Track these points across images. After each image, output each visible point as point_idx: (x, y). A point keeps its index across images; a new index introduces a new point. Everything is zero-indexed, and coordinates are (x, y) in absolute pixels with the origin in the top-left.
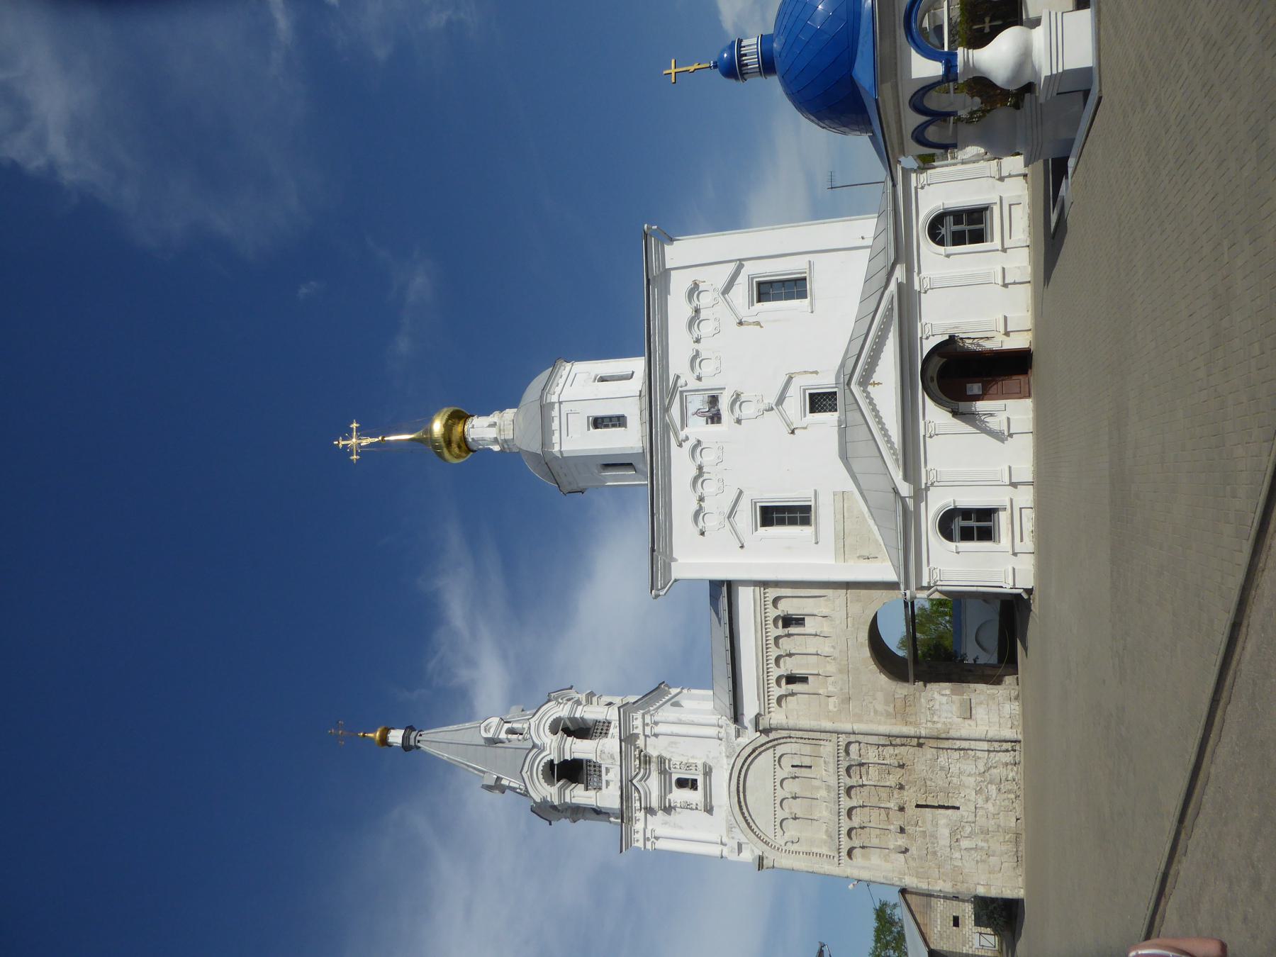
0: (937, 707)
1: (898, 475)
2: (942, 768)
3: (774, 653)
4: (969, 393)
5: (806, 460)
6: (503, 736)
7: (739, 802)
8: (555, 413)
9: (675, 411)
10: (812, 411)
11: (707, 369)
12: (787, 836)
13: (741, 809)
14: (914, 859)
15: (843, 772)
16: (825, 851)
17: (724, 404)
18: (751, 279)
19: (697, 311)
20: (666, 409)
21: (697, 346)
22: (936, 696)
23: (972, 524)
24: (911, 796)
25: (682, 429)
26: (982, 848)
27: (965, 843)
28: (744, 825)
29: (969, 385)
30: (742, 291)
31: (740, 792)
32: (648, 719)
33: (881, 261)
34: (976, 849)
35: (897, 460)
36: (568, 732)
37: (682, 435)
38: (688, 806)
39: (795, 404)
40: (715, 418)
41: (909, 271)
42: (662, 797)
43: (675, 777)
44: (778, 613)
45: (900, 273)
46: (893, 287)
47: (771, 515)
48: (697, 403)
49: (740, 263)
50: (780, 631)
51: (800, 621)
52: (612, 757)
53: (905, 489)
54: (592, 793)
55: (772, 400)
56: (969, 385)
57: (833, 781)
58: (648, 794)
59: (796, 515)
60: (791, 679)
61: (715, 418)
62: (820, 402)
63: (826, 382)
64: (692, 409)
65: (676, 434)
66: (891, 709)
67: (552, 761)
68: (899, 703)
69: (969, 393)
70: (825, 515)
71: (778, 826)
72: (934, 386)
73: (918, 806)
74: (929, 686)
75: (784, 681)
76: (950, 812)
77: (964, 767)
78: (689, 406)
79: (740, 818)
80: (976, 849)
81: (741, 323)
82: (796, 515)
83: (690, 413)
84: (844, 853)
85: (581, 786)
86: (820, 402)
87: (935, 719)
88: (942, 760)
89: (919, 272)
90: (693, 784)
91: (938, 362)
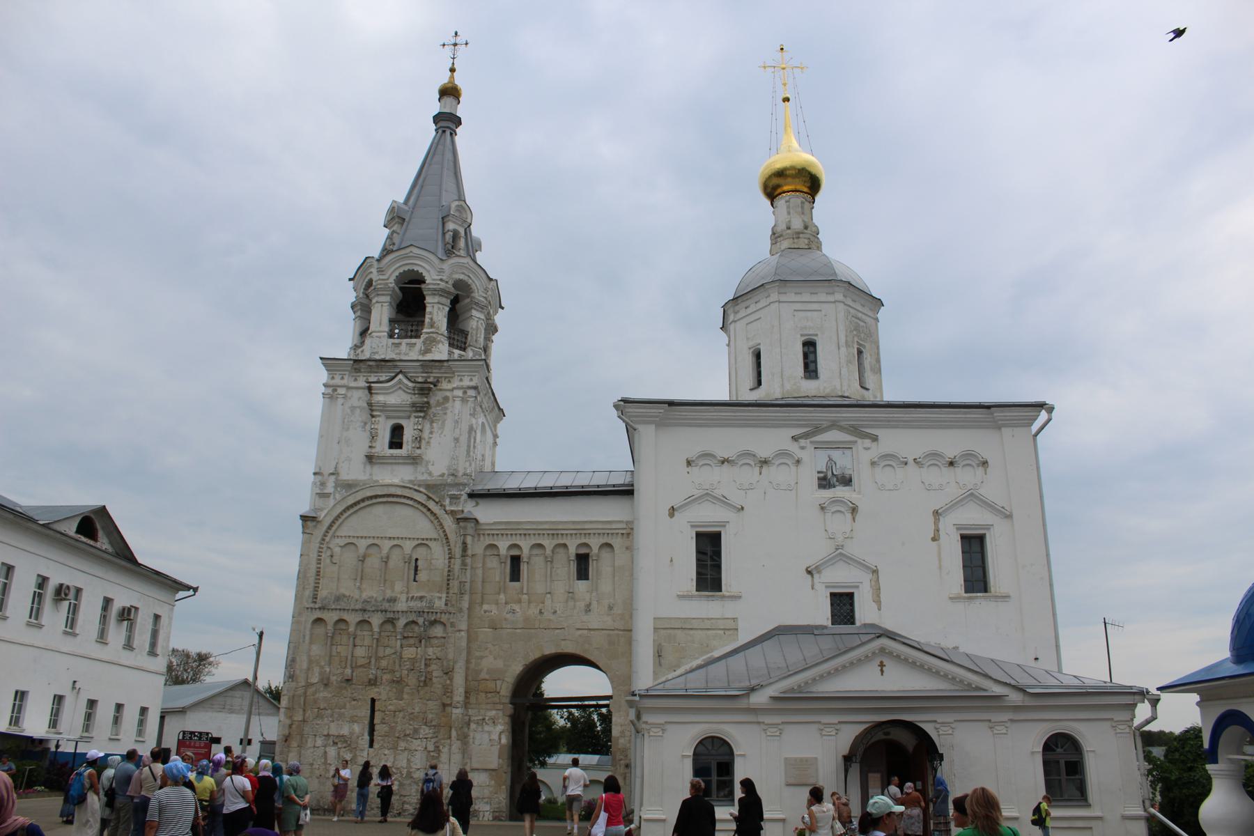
0: (487, 728)
1: (772, 691)
2: (416, 731)
3: (548, 543)
5: (773, 587)
6: (451, 226)
7: (376, 497)
8: (823, 297)
9: (834, 436)
12: (337, 550)
13: (371, 498)
14: (315, 693)
15: (412, 617)
16: (323, 593)
17: (840, 492)
18: (988, 527)
19: (951, 464)
20: (834, 425)
21: (911, 461)
22: (500, 728)
24: (382, 693)
26: (327, 771)
27: (332, 752)
28: (351, 501)
29: (878, 775)
30: (972, 517)
31: (388, 498)
32: (471, 393)
33: (1024, 680)
34: (325, 763)
35: (792, 690)
36: (455, 301)
38: (373, 437)
39: (841, 577)
40: (825, 482)
41: (1016, 708)
42: (384, 408)
43: (403, 422)
44: (595, 550)
45: (1015, 698)
46: (997, 690)
47: (709, 548)
48: (843, 462)
49: (1009, 516)
50: (572, 551)
51: (583, 574)
52: (427, 351)
54: (386, 327)
56: (878, 775)
57: (401, 606)
58: (387, 392)
60: (516, 561)
61: (825, 482)
62: (843, 605)
63: (865, 612)
64: (836, 455)
65: (805, 436)
66: (483, 675)
67: (424, 282)
68: (491, 685)
70: (707, 608)
71: (348, 541)
72: (880, 736)
73: (373, 701)
74: (507, 719)
75: (515, 552)
76: (367, 737)
77: (418, 755)
78: (839, 452)
79: (359, 496)
80: (325, 763)
81: (936, 513)
84: (318, 614)
85: (393, 316)
86: (843, 605)
87: (473, 726)
88: (425, 731)
89: (1012, 721)
90: (396, 443)
91: (908, 741)
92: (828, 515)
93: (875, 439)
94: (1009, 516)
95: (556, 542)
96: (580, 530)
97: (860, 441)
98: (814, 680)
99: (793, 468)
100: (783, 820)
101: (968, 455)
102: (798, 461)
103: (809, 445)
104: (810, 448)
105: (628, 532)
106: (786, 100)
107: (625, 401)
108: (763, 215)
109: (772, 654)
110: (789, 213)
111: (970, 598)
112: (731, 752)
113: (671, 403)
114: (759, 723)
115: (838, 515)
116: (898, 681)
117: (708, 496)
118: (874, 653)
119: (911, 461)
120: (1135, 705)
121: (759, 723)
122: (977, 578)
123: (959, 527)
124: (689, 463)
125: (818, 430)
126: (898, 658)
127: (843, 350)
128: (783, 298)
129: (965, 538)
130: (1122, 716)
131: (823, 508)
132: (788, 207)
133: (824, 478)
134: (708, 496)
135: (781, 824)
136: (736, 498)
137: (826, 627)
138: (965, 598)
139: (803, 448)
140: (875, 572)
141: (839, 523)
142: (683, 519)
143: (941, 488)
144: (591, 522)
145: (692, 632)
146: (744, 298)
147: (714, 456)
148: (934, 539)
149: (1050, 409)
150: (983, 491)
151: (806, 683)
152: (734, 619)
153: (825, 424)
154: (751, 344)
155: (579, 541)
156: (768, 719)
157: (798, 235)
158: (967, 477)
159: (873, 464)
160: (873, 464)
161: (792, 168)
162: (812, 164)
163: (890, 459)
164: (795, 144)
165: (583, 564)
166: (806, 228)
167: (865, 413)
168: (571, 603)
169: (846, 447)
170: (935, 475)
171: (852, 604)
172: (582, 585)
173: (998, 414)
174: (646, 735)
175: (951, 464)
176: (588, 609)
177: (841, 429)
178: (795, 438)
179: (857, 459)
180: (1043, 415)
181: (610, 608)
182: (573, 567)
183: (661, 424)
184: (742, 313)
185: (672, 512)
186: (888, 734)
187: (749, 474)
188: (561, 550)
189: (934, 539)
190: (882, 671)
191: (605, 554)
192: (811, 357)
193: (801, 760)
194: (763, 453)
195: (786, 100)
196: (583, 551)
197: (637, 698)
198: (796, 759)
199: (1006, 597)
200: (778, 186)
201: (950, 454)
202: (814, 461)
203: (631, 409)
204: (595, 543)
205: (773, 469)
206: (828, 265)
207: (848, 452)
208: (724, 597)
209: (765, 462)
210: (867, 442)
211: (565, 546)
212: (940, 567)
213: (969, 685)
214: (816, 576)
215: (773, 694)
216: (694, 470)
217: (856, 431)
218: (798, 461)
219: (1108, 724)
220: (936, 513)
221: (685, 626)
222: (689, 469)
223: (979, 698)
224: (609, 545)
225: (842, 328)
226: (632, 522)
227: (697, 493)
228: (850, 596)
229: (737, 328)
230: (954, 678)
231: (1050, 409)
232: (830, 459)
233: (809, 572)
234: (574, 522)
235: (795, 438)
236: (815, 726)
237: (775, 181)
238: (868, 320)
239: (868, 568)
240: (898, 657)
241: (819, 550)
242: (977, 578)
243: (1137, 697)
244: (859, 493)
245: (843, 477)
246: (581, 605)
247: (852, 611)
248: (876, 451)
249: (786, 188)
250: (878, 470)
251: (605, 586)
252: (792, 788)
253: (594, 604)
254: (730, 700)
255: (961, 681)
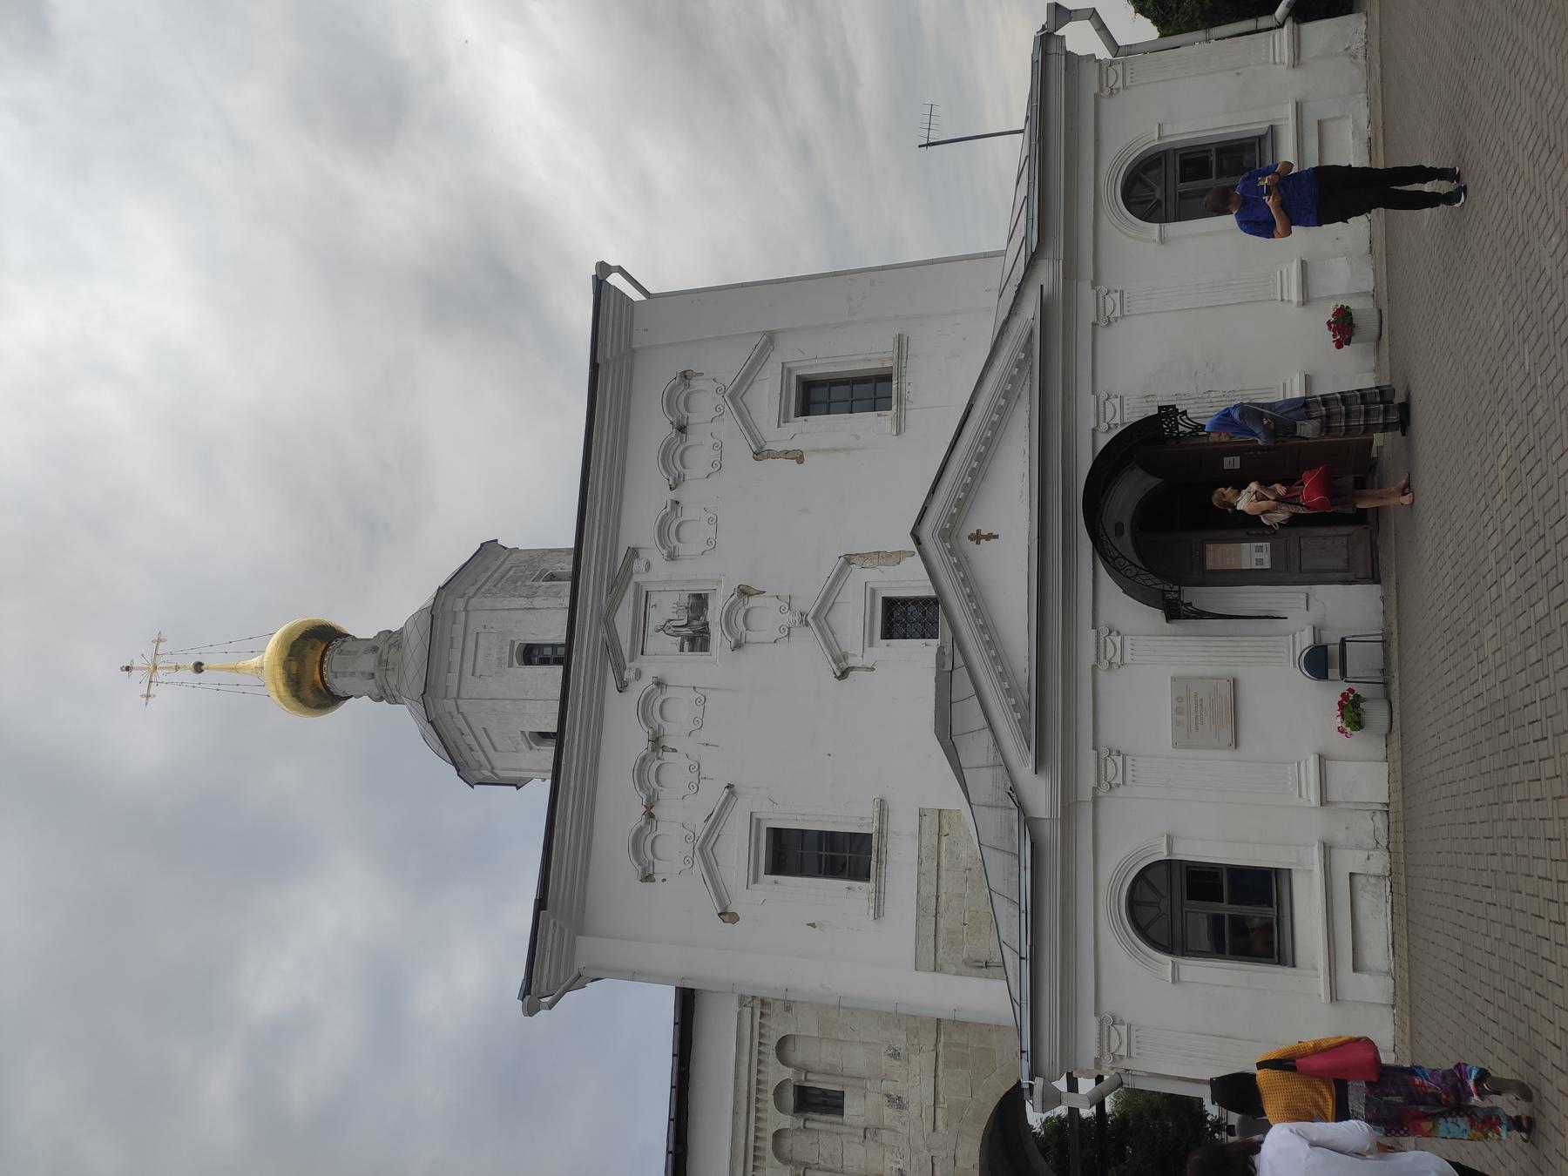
4: (1210, 565)
5: (873, 740)
10: (888, 634)
11: (693, 538)
18: (786, 371)
19: (682, 429)
20: (607, 620)
21: (672, 495)
23: (1219, 910)
25: (632, 660)
30: (768, 396)
37: (629, 675)
39: (854, 618)
40: (698, 640)
41: (1070, 273)
44: (788, 1073)
45: (1047, 274)
47: (797, 853)
48: (667, 608)
50: (786, 1121)
51: (831, 1103)
53: (1040, 795)
55: (810, 607)
59: (840, 856)
61: (698, 640)
62: (902, 618)
64: (656, 619)
65: (619, 668)
69: (1210, 565)
72: (1125, 544)
78: (652, 613)
81: (758, 455)
82: (840, 856)
83: (651, 627)
86: (902, 618)
91: (1133, 488)
92: (751, 636)
93: (634, 553)
94: (770, 338)
95: (769, 1153)
96: (750, 1100)
97: (636, 578)
98: (1002, 676)
99: (670, 692)
100: (1322, 760)
101: (670, 402)
102: (659, 683)
103: (635, 665)
104: (641, 662)
105: (760, 1006)
106: (198, 667)
107: (527, 990)
108: (358, 712)
109: (976, 750)
110: (352, 674)
111: (899, 402)
112: (1169, 863)
113: (541, 904)
114: (1096, 799)
115: (752, 619)
116: (1009, 506)
117: (706, 849)
118: (952, 552)
119: (672, 495)
120: (1069, 55)
121: (1096, 799)
122: (869, 391)
123: (784, 419)
124: (648, 878)
125: (611, 648)
126: (963, 505)
127: (537, 602)
128: (453, 692)
129: (805, 409)
130: (1090, 83)
131: (738, 646)
132: (344, 674)
133: (692, 640)
134: (706, 849)
135: (1334, 768)
136: (712, 795)
137: (941, 649)
138: (899, 410)
139: (639, 675)
140: (848, 560)
141: (766, 617)
142: (743, 899)
143: (719, 447)
144: (737, 1077)
145: (943, 898)
146: (454, 751)
147: (639, 831)
148: (800, 460)
149: (604, 269)
150: (729, 378)
151: (1009, 692)
152: (922, 814)
153: (603, 634)
154: (523, 746)
155: (771, 1104)
156: (1087, 779)
157: (383, 663)
158: (705, 405)
159: (672, 557)
160: (672, 557)
161: (286, 666)
162: (285, 637)
163: (668, 529)
164: (256, 661)
165: (815, 1101)
166: (375, 649)
167: (592, 568)
168: (885, 1136)
169: (644, 601)
170: (699, 458)
171: (905, 602)
172: (852, 1106)
173: (606, 353)
174: (1127, 1064)
175: (682, 429)
176: (897, 1102)
177: (613, 607)
178: (622, 687)
179: (665, 583)
180: (615, 280)
181: (895, 1055)
182: (819, 1122)
183: (579, 923)
184: (480, 756)
185: (727, 916)
186: (1119, 529)
187: (675, 770)
188: (787, 1142)
189: (800, 460)
190: (990, 537)
191: (799, 1053)
192: (548, 652)
193: (1177, 711)
194: (641, 744)
195: (198, 667)
196: (790, 1099)
197: (1038, 1083)
198: (1176, 723)
199: (901, 342)
200: (314, 684)
201: (666, 430)
202: (663, 656)
203: (543, 980)
204: (776, 1073)
205: (668, 728)
206: (415, 618)
207: (653, 599)
208: (880, 832)
209: (656, 742)
210: (638, 565)
211: (778, 1135)
212: (847, 450)
213: (1019, 364)
214: (851, 662)
215: (1031, 766)
216: (660, 868)
217: (618, 583)
218: (659, 683)
219: (1106, 104)
220: (758, 455)
221: (931, 909)
222: (658, 878)
223: (1048, 342)
224: (782, 1043)
225: (506, 603)
226: (742, 998)
227: (699, 867)
228: (890, 604)
229: (504, 764)
230: (1007, 395)
231: (604, 269)
232: (663, 629)
233: (844, 674)
234: (735, 1112)
235: (622, 687)
236: (1102, 675)
237: (307, 693)
238: (507, 564)
239: (841, 571)
240: (960, 504)
241: (808, 650)
242: (869, 391)
243: (1053, 49)
244: (719, 582)
245: (691, 608)
246: (889, 1113)
247: (915, 601)
248: (653, 552)
249: (318, 677)
250: (683, 550)
251: (856, 1059)
252: (1245, 736)
253: (888, 1086)
254: (1043, 857)
255: (1013, 380)
